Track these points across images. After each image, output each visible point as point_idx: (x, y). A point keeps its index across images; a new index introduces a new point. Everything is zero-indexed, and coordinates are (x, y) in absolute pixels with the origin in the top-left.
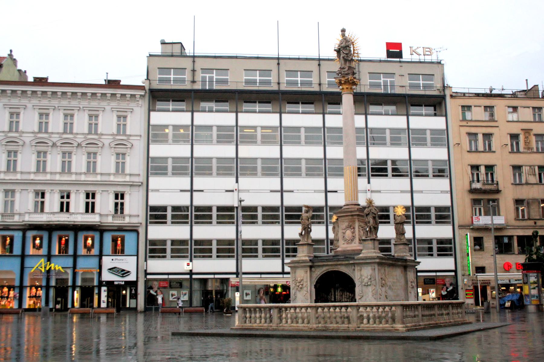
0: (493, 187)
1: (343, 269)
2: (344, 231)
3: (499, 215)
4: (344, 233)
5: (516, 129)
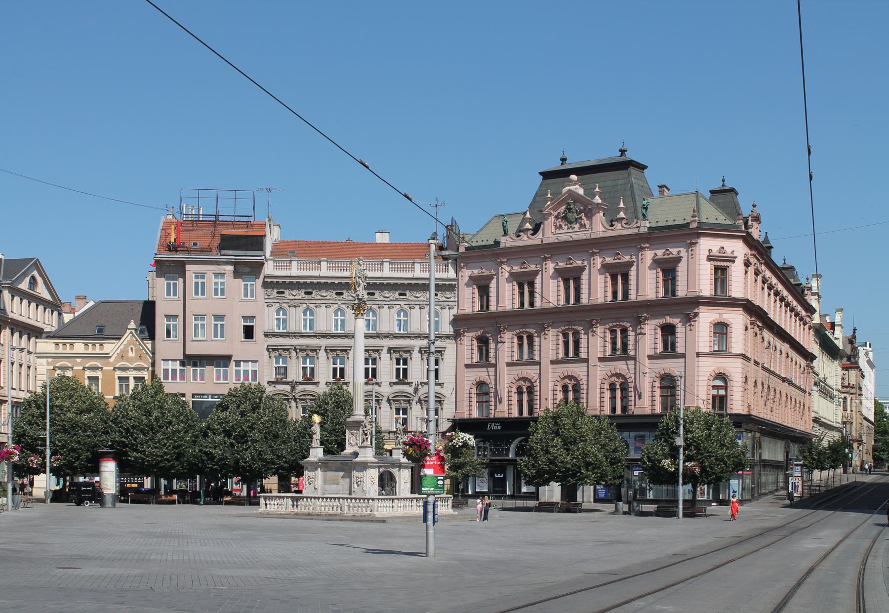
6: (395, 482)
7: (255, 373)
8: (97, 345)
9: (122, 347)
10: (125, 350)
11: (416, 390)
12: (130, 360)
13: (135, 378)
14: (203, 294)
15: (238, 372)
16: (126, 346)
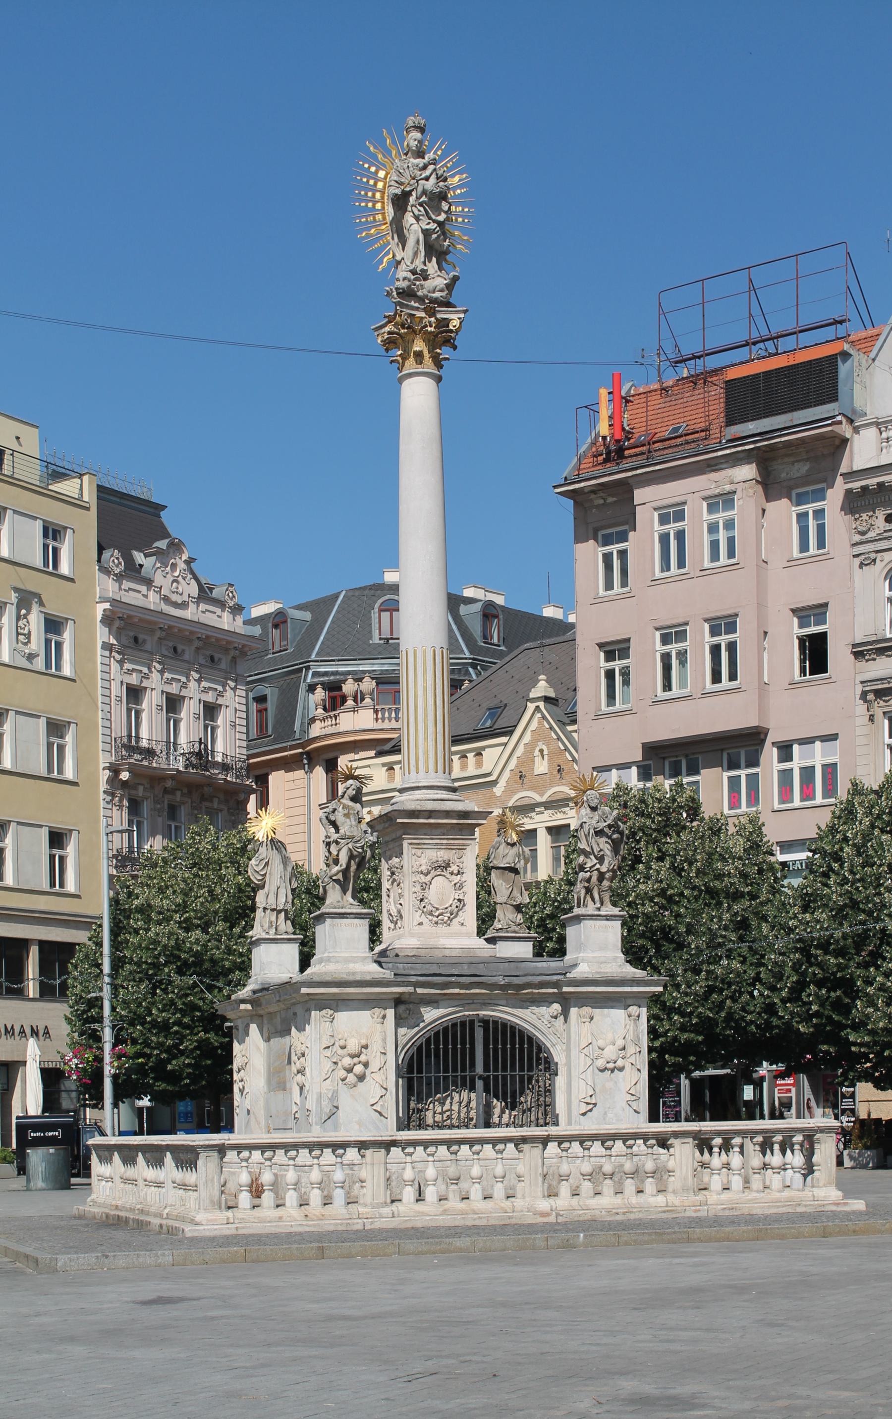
2: (424, 879)
4: (425, 887)
6: (550, 1067)
7: (830, 770)
8: (470, 756)
10: (528, 760)
13: (549, 829)
14: (681, 564)
15: (786, 776)
16: (530, 747)
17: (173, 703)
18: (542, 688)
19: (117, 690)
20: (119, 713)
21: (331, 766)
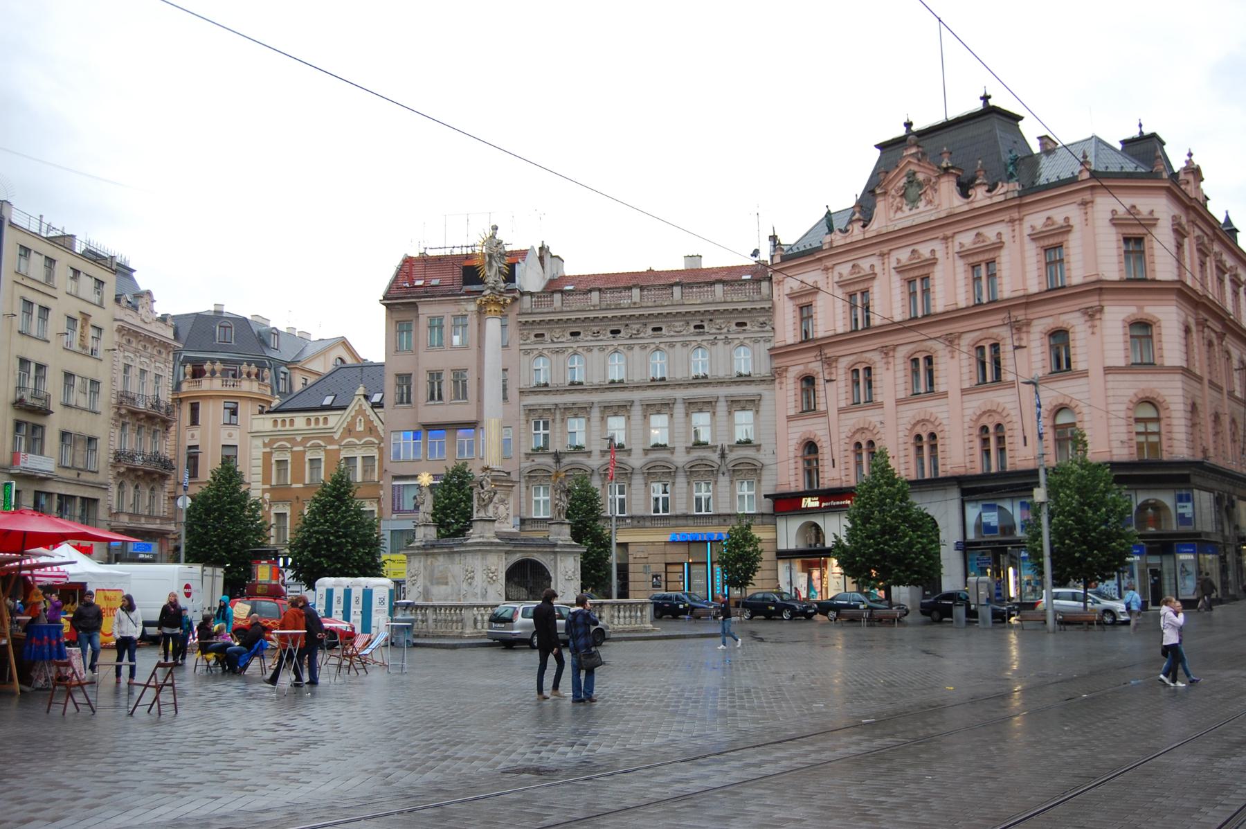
0: (38, 404)
1: (538, 558)
3: (42, 453)
5: (74, 308)
6: (549, 579)
9: (349, 419)
11: (723, 456)
12: (359, 435)
16: (354, 418)
17: (143, 372)
18: (361, 390)
19: (122, 367)
20: (120, 377)
21: (195, 409)
